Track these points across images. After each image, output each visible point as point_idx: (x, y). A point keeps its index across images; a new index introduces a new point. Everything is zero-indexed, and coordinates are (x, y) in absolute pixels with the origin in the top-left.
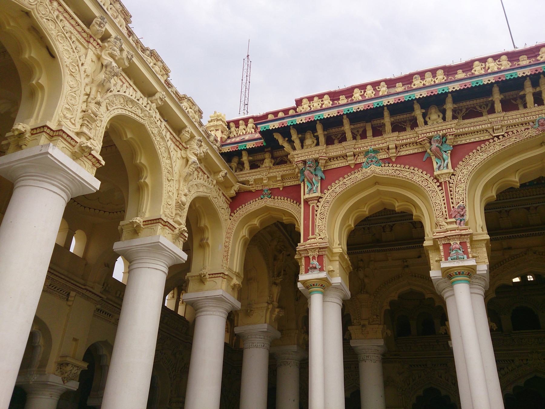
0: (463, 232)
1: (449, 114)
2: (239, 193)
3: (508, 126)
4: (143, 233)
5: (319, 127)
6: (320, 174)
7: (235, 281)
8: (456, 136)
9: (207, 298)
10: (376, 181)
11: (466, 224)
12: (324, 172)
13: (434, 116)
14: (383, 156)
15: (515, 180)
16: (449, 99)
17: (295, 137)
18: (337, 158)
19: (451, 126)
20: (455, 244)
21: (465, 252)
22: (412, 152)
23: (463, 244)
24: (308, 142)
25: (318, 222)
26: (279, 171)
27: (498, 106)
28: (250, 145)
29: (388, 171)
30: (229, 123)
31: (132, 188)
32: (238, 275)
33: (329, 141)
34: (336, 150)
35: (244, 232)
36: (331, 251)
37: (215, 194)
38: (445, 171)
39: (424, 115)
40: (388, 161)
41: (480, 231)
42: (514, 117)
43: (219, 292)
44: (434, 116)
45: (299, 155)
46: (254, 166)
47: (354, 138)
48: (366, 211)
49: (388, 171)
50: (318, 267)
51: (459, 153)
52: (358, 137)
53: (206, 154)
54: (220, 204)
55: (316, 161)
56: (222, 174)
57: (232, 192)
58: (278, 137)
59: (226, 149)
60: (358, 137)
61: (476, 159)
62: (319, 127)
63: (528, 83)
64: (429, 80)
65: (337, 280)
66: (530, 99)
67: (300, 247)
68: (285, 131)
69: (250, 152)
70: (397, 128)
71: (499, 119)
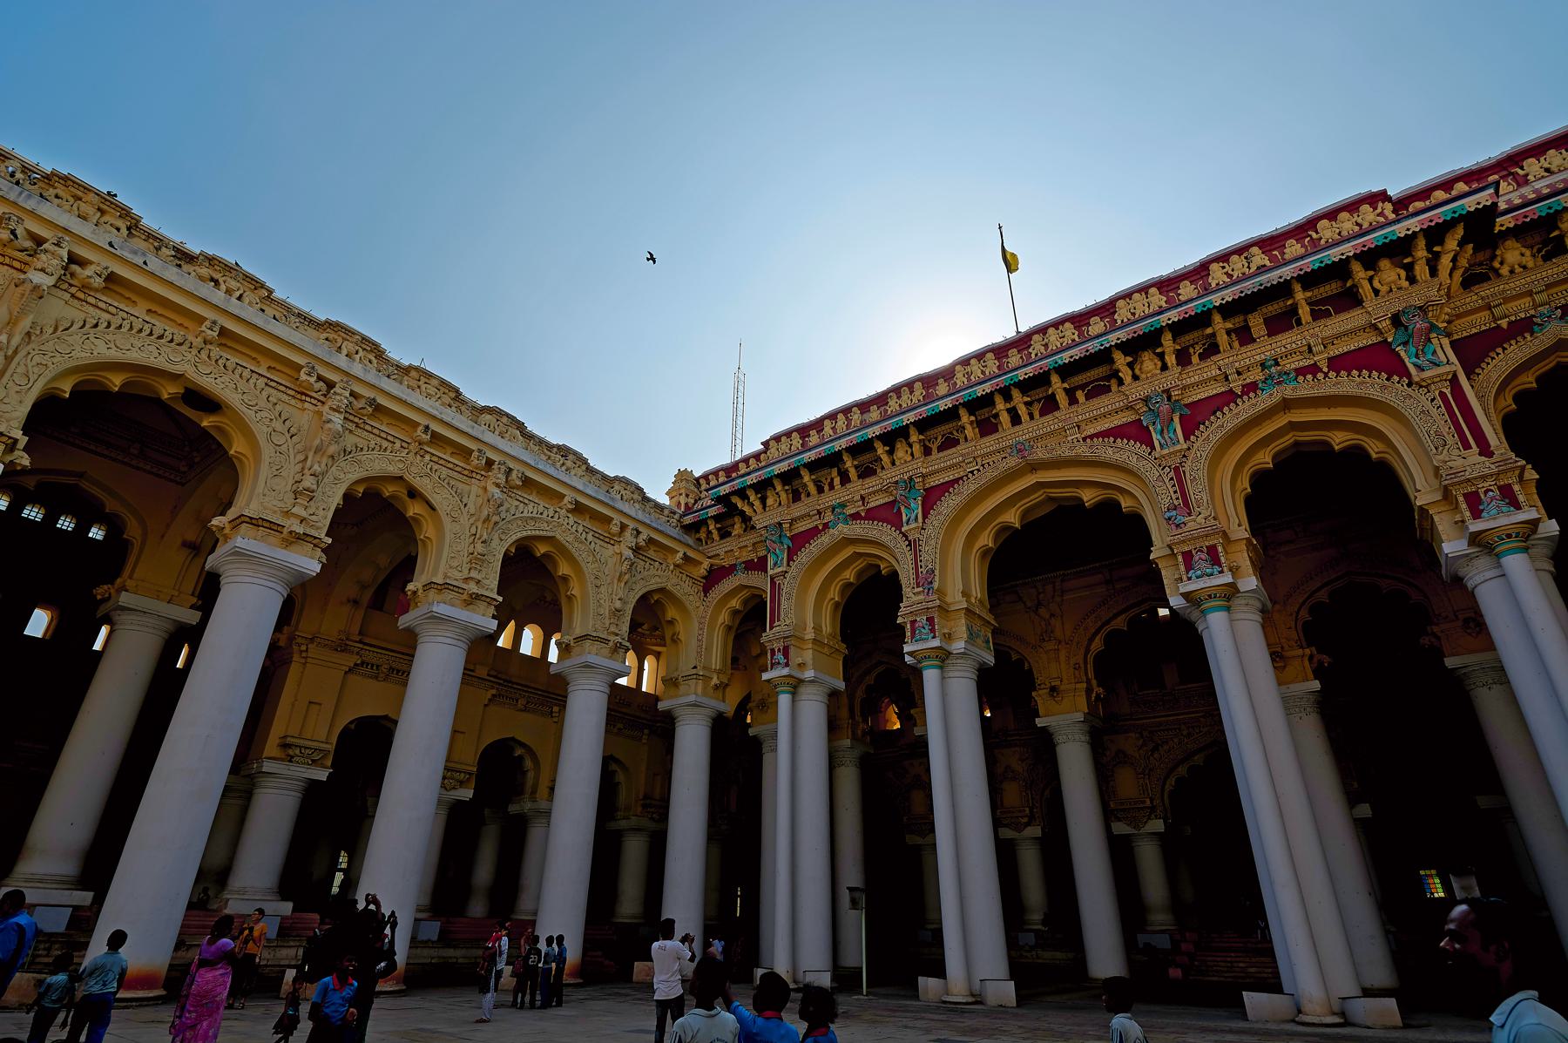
0: (930, 605)
2: (711, 571)
3: (983, 456)
4: (576, 650)
5: (777, 483)
6: (787, 542)
7: (715, 681)
8: (924, 476)
9: (681, 705)
11: (941, 593)
12: (792, 538)
14: (850, 511)
15: (1012, 518)
16: (912, 431)
18: (802, 517)
21: (933, 630)
22: (882, 502)
23: (930, 620)
24: (770, 501)
26: (749, 539)
27: (969, 432)
28: (713, 512)
30: (697, 480)
31: (563, 601)
32: (719, 672)
33: (796, 497)
34: (798, 509)
35: (724, 617)
36: (802, 639)
37: (675, 581)
38: (913, 525)
39: (891, 452)
40: (856, 516)
41: (959, 597)
42: (990, 443)
43: (692, 698)
44: (901, 452)
45: (761, 520)
46: (725, 534)
47: (820, 490)
48: (849, 575)
50: (783, 661)
51: (932, 497)
52: (826, 488)
53: (651, 541)
54: (685, 589)
55: (780, 524)
56: (680, 555)
57: (702, 570)
58: (735, 500)
59: (688, 520)
60: (826, 488)
62: (777, 483)
63: (999, 399)
64: (905, 399)
66: (1005, 418)
67: (768, 636)
68: (741, 493)
69: (717, 518)
70: (866, 472)
71: (974, 446)
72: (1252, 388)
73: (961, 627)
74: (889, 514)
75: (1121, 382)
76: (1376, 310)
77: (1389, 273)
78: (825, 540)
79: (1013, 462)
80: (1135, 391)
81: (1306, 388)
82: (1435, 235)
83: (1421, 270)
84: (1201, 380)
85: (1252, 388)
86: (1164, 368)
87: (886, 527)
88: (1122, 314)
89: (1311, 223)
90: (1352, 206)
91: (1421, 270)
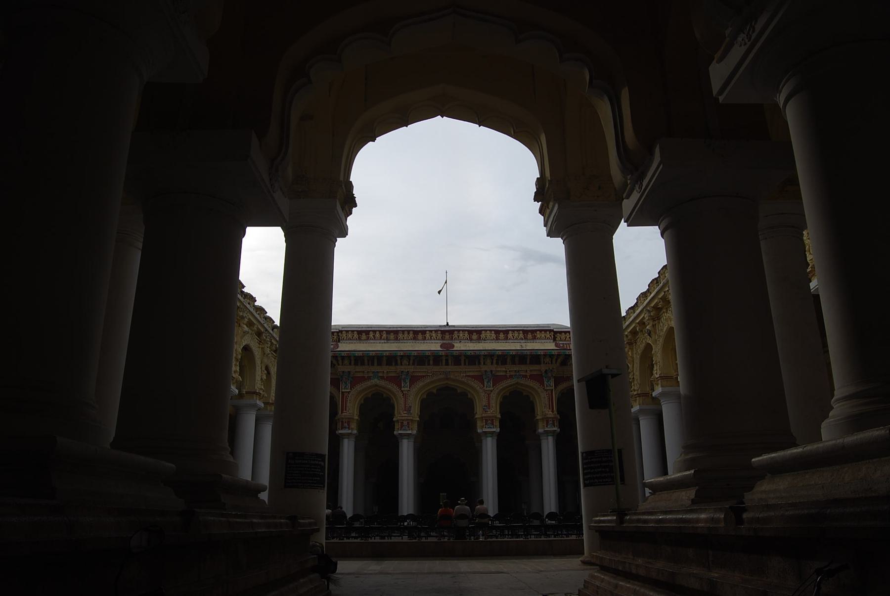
1: (411, 362)
10: (376, 385)
13: (405, 362)
14: (381, 375)
17: (339, 359)
19: (411, 369)
20: (405, 423)
24: (346, 362)
25: (348, 404)
27: (431, 362)
29: (382, 383)
34: (359, 368)
40: (382, 378)
42: (436, 368)
44: (405, 362)
49: (382, 383)
61: (420, 384)
65: (355, 432)
72: (511, 377)
73: (415, 426)
74: (397, 380)
75: (479, 363)
76: (543, 367)
77: (548, 360)
78: (369, 383)
79: (442, 376)
80: (484, 368)
81: (522, 381)
82: (559, 355)
83: (554, 361)
84: (501, 370)
85: (511, 377)
86: (492, 363)
87: (395, 387)
88: (483, 336)
89: (536, 331)
90: (546, 331)
91: (554, 361)
